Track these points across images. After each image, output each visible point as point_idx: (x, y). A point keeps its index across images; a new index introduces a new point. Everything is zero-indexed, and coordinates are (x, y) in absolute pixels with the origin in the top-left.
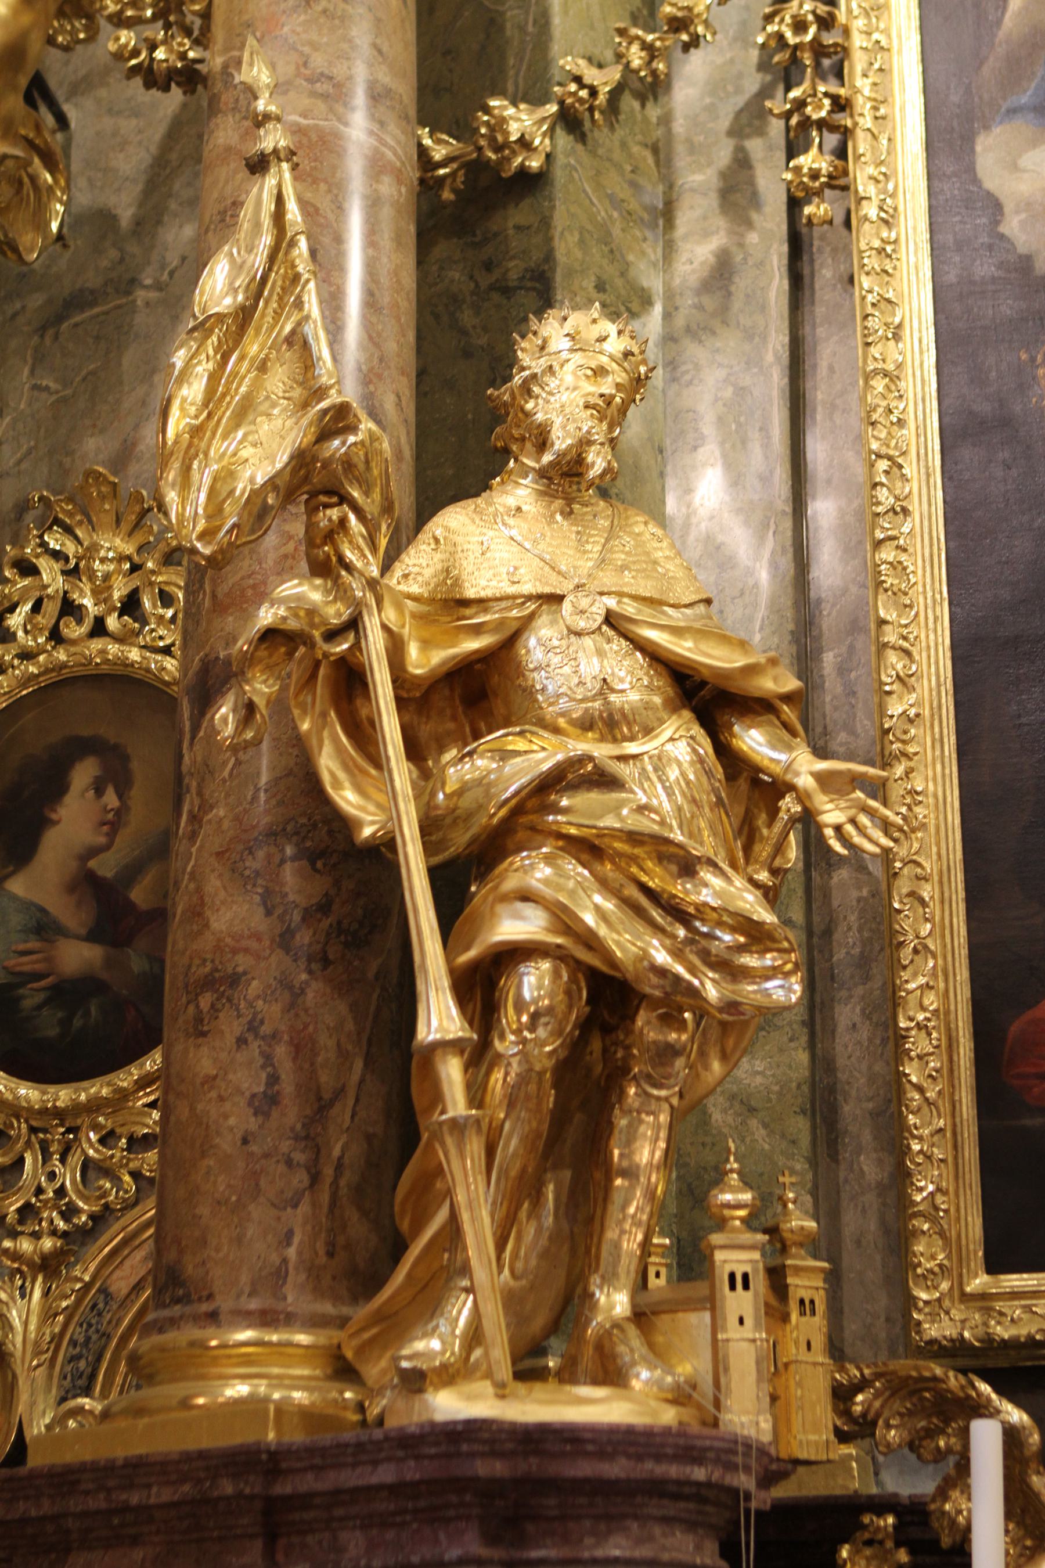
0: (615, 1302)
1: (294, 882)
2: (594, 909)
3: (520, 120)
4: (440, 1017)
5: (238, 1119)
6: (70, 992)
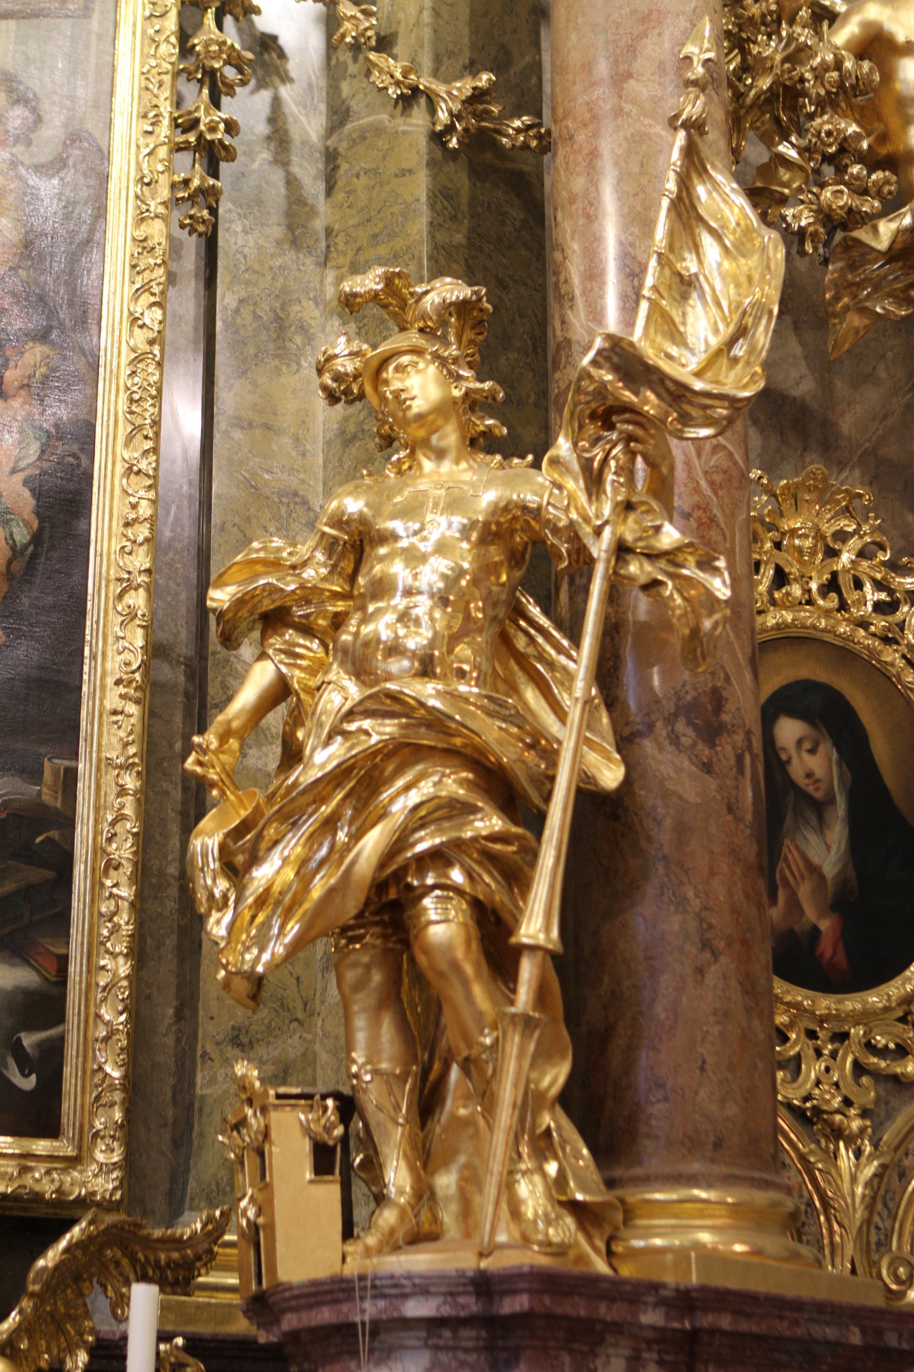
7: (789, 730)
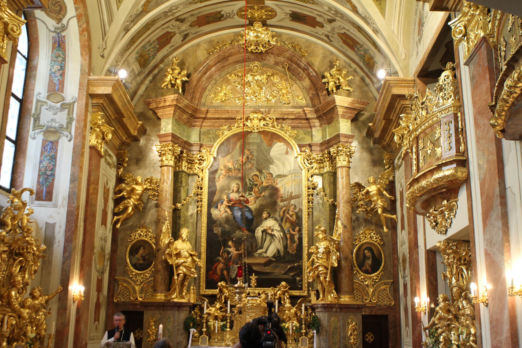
0: (184, 294)
1: (164, 265)
2: (185, 270)
3: (179, 205)
4: (176, 277)
5: (160, 280)
6: (141, 264)
7: (366, 251)
